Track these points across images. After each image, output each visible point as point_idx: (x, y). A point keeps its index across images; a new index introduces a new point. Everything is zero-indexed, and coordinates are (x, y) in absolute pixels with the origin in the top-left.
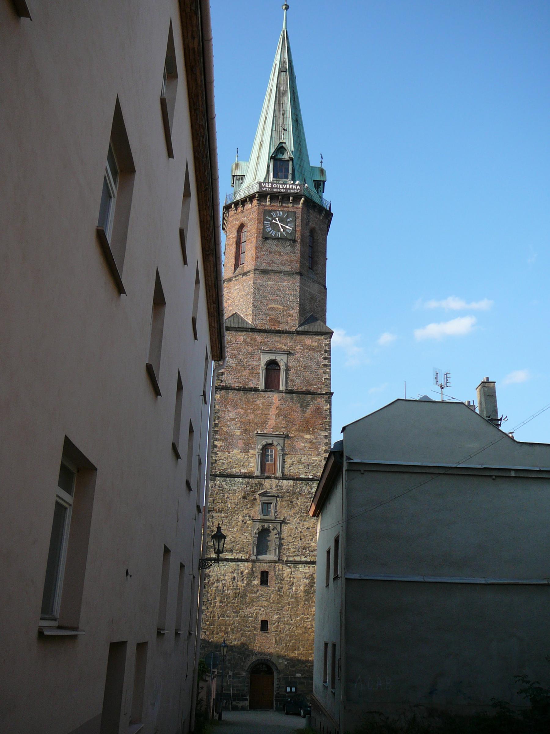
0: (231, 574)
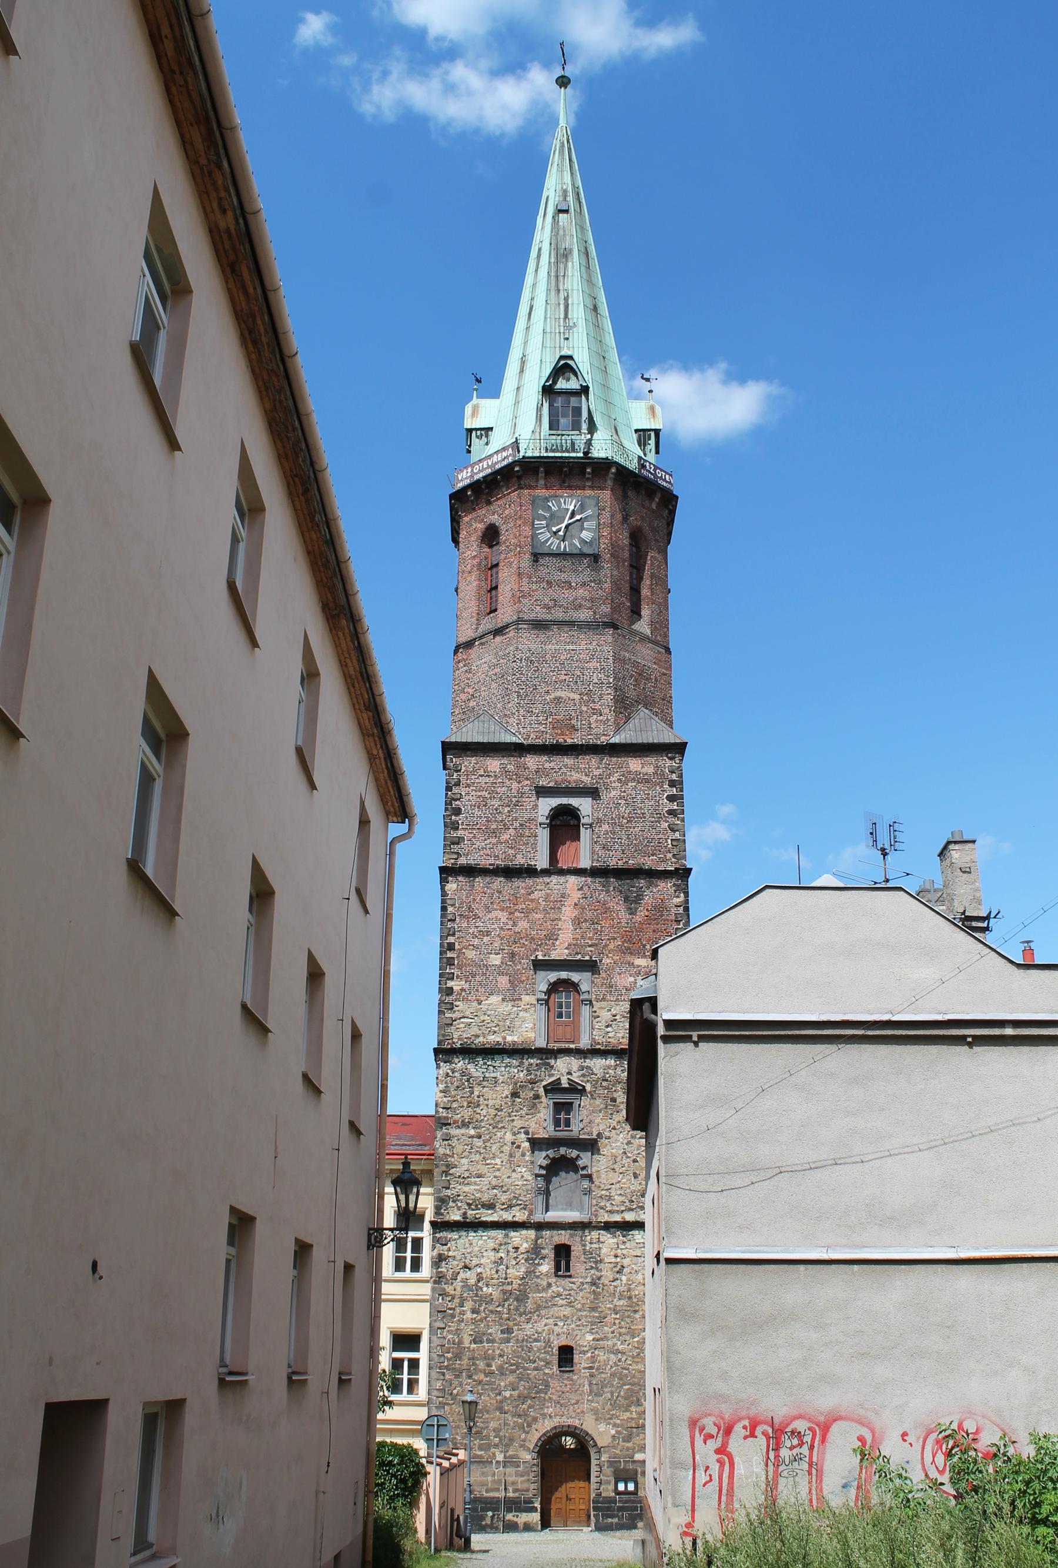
0: (492, 1253)
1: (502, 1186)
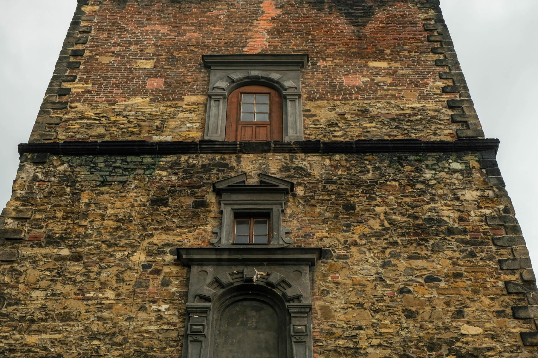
1: (114, 334)
